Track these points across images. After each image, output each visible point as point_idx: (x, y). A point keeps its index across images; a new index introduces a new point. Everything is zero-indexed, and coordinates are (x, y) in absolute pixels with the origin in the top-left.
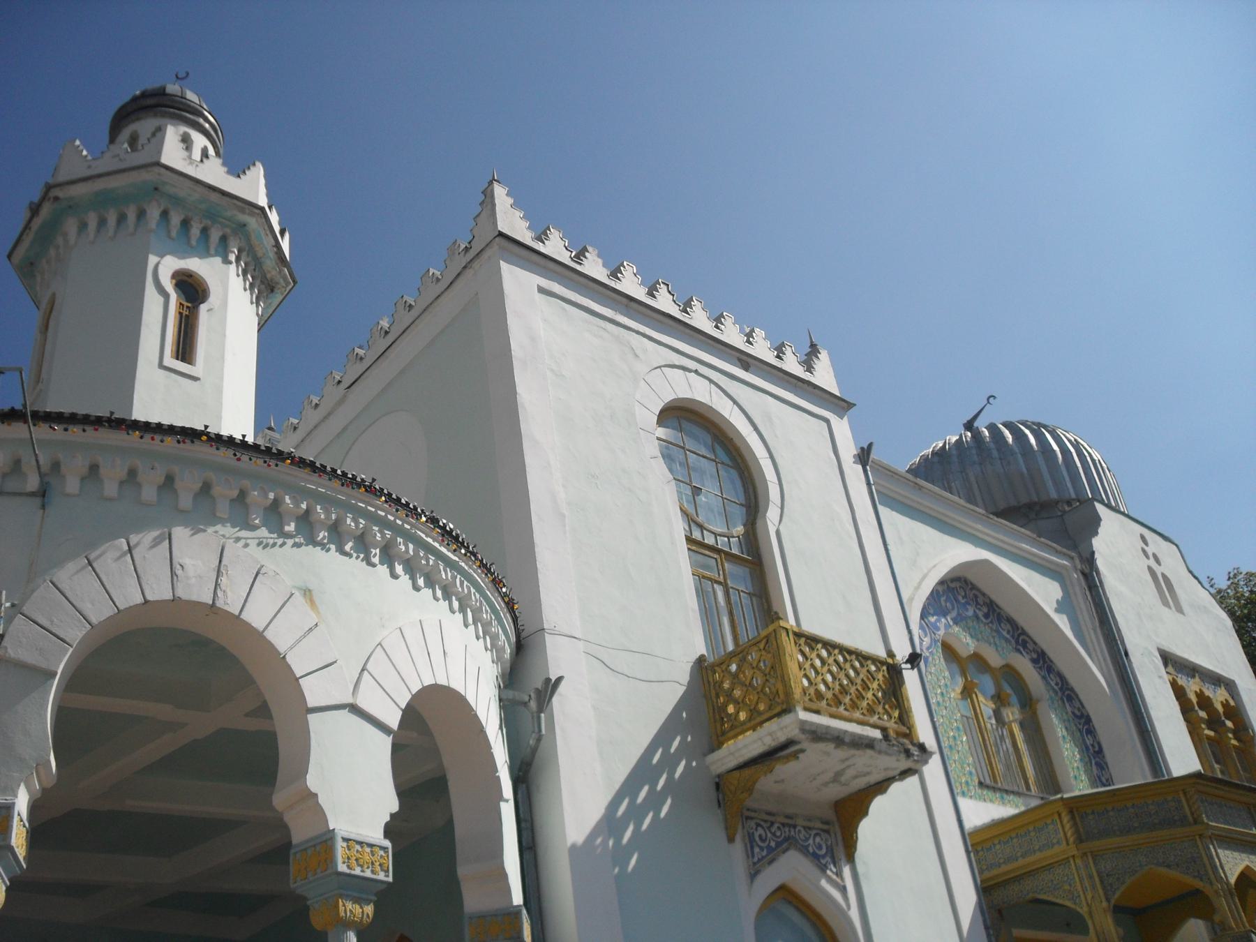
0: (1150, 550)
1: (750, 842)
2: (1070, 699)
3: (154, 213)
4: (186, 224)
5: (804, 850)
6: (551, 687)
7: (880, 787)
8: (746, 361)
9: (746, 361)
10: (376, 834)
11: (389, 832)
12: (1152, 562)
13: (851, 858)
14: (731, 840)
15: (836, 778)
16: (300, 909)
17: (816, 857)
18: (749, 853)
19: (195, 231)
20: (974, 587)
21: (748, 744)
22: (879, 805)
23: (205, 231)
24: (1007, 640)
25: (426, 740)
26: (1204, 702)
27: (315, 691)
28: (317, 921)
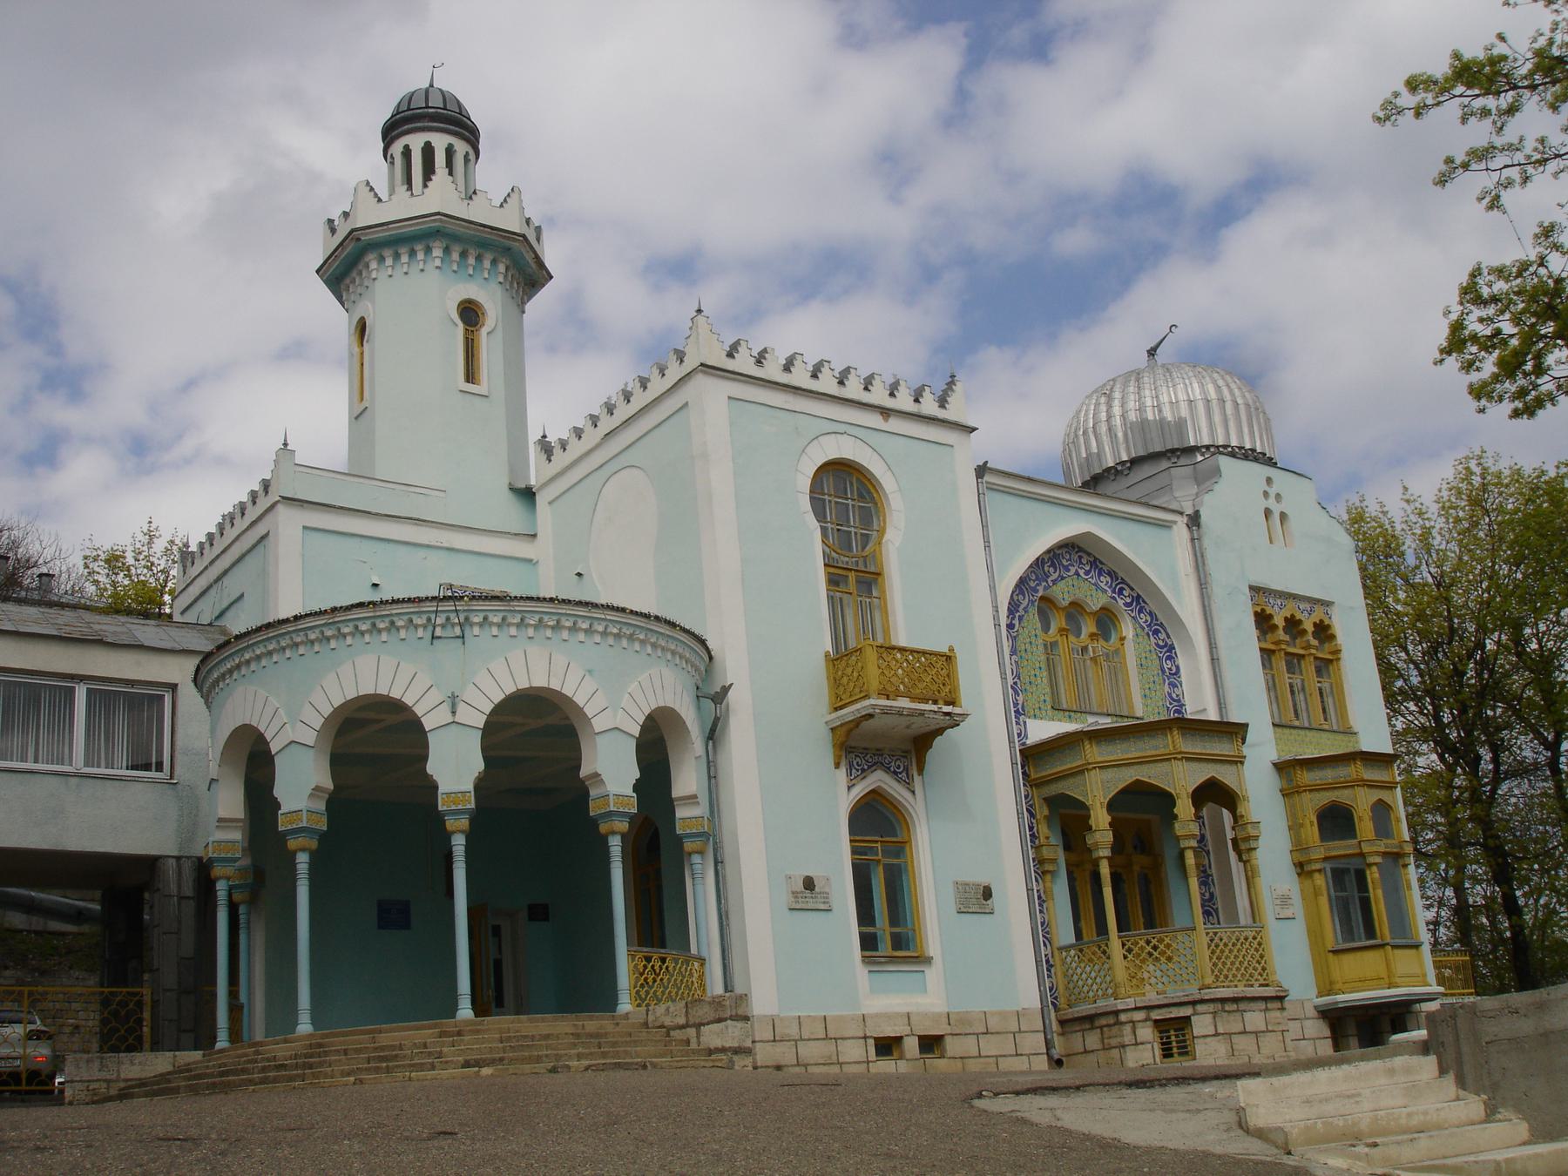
0: (1272, 492)
1: (851, 766)
2: (1156, 632)
3: (437, 252)
4: (464, 255)
5: (887, 770)
6: (726, 690)
7: (940, 731)
8: (886, 412)
9: (886, 412)
10: (629, 791)
11: (636, 788)
12: (1272, 499)
13: (921, 771)
14: (837, 766)
15: (908, 727)
16: (594, 823)
17: (895, 773)
18: (849, 773)
19: (471, 261)
20: (1080, 549)
21: (849, 713)
22: (938, 741)
23: (479, 258)
24: (1105, 591)
25: (655, 745)
26: (1293, 624)
27: (599, 724)
28: (603, 828)
